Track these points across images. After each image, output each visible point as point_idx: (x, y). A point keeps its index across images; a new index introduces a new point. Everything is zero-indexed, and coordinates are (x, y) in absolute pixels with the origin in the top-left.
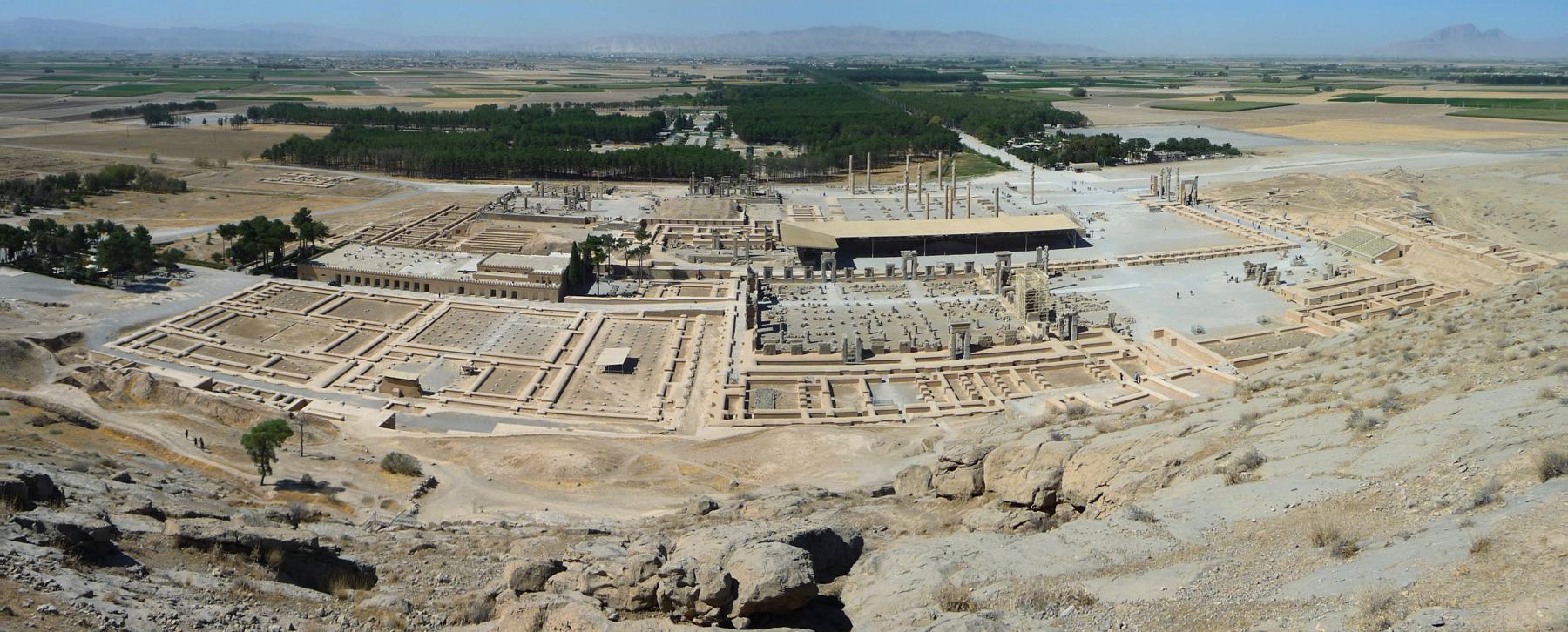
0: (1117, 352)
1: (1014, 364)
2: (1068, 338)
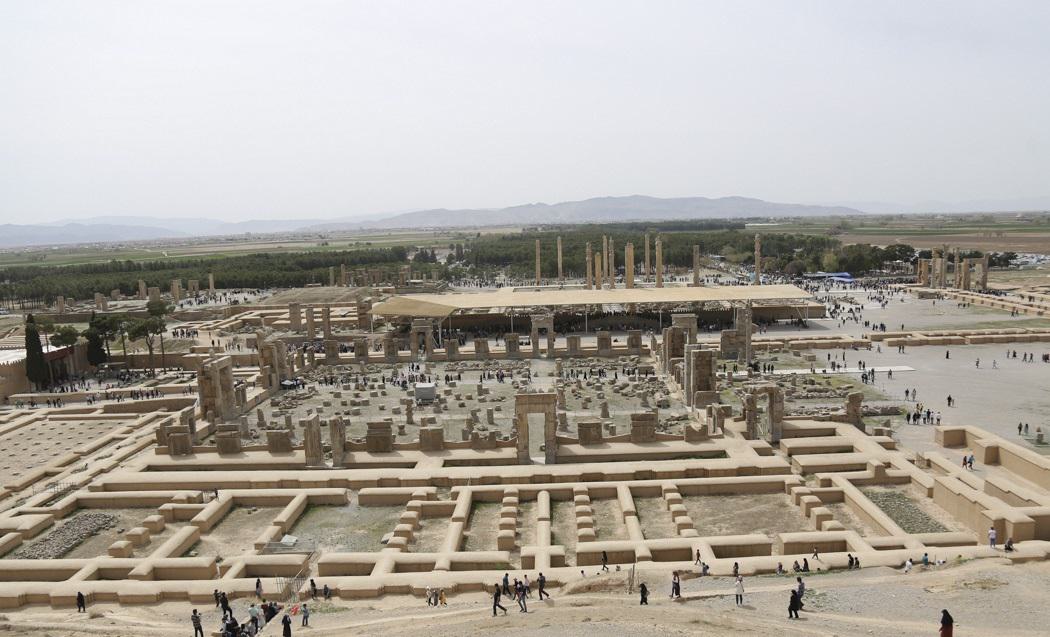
1: (638, 476)
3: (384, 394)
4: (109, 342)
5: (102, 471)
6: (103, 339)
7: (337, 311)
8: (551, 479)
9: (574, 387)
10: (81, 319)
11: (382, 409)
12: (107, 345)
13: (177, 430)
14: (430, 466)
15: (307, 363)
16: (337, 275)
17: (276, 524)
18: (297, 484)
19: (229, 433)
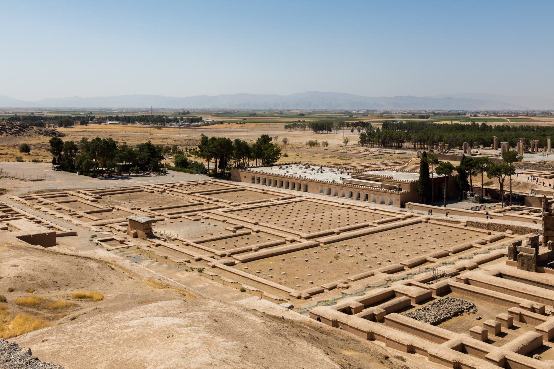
4: (472, 177)
5: (464, 269)
6: (468, 174)
10: (455, 158)
12: (471, 178)
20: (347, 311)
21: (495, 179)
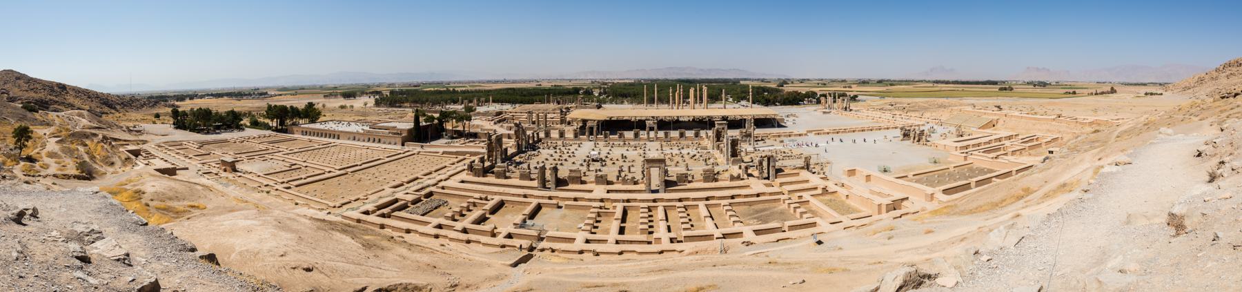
0: (816, 188)
1: (707, 199)
2: (768, 178)
3: (574, 156)
7: (549, 116)
8: (662, 200)
9: (670, 156)
11: (574, 163)
13: (478, 165)
14: (600, 191)
15: (536, 139)
16: (549, 97)
17: (524, 215)
18: (532, 196)
19: (501, 169)
20: (367, 213)
21: (460, 124)
